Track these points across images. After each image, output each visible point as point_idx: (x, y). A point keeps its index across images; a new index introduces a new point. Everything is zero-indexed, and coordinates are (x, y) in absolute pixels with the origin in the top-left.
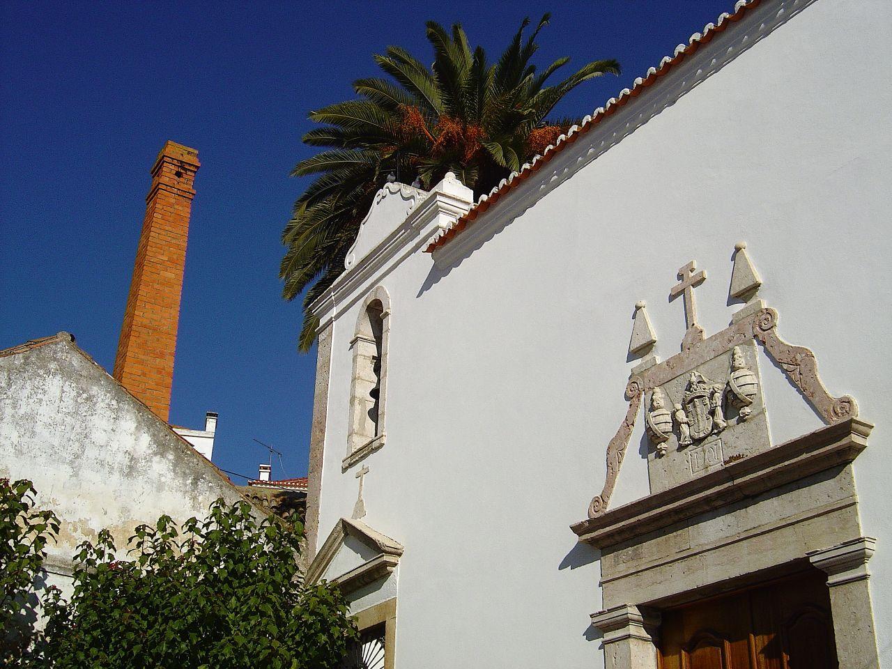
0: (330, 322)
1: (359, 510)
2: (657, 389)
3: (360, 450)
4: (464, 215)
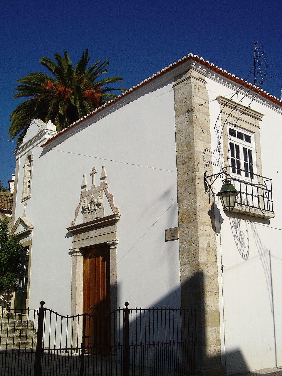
0: (19, 158)
1: (24, 215)
2: (86, 198)
3: (25, 198)
4: (52, 137)
